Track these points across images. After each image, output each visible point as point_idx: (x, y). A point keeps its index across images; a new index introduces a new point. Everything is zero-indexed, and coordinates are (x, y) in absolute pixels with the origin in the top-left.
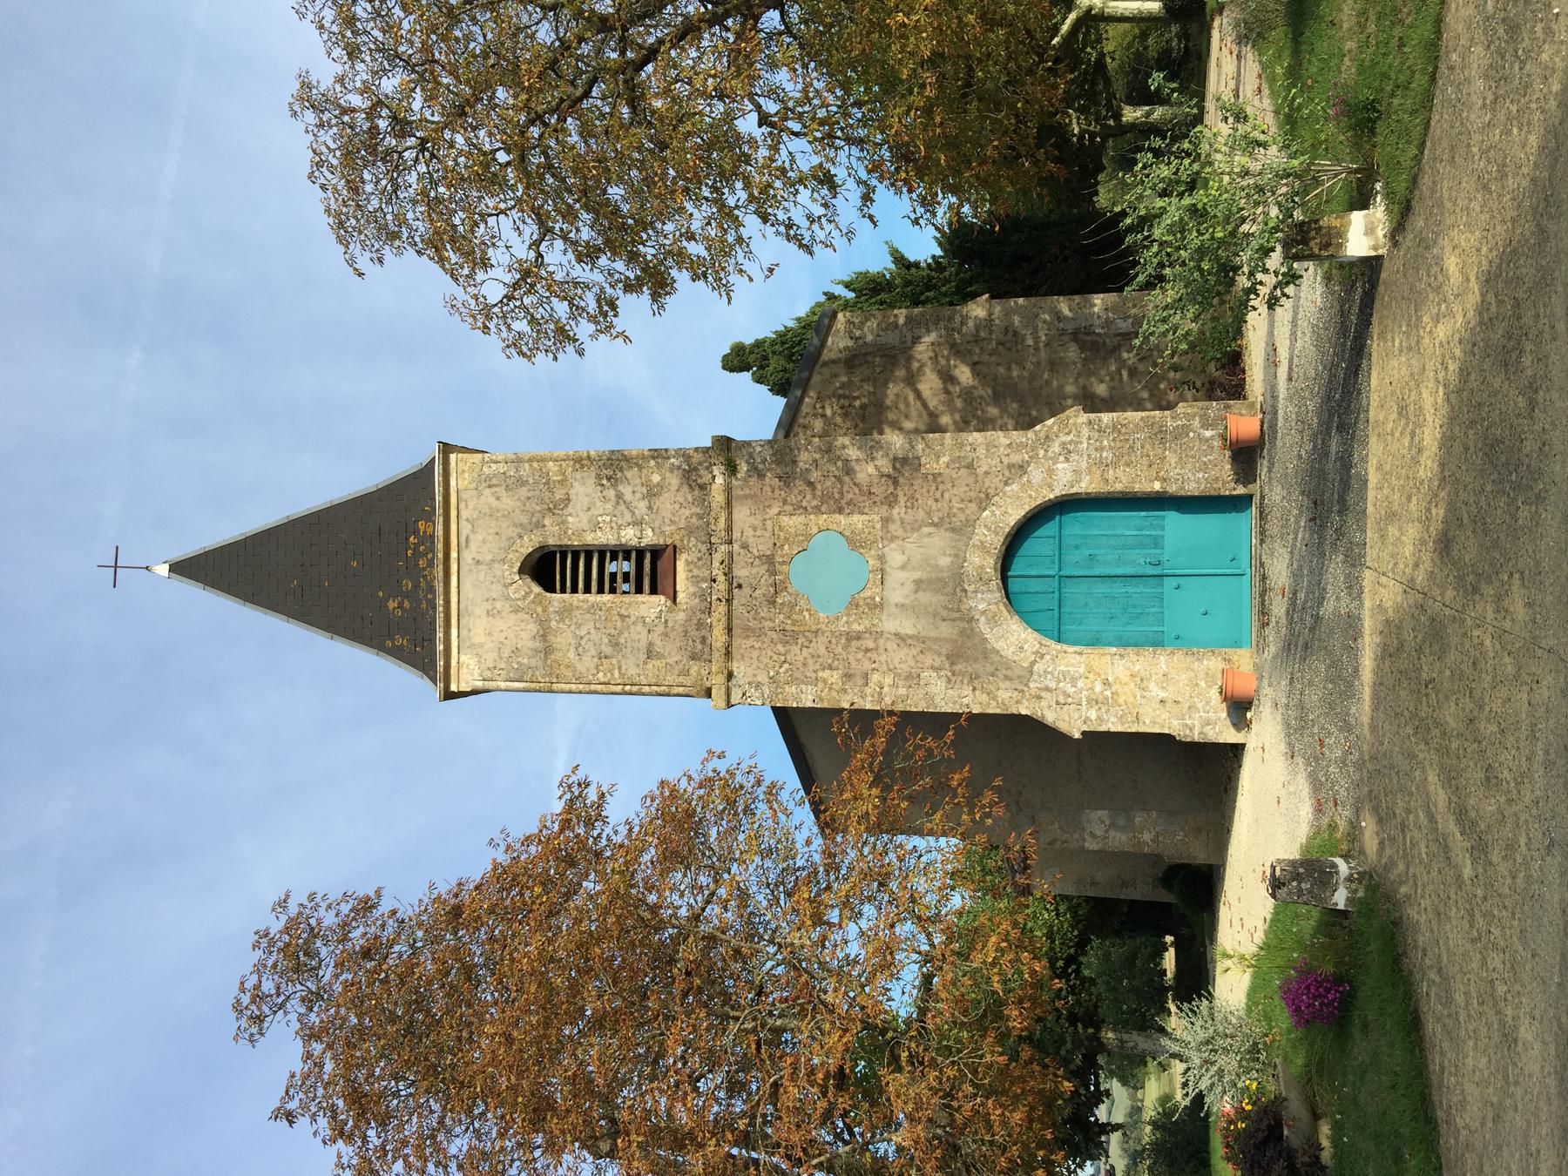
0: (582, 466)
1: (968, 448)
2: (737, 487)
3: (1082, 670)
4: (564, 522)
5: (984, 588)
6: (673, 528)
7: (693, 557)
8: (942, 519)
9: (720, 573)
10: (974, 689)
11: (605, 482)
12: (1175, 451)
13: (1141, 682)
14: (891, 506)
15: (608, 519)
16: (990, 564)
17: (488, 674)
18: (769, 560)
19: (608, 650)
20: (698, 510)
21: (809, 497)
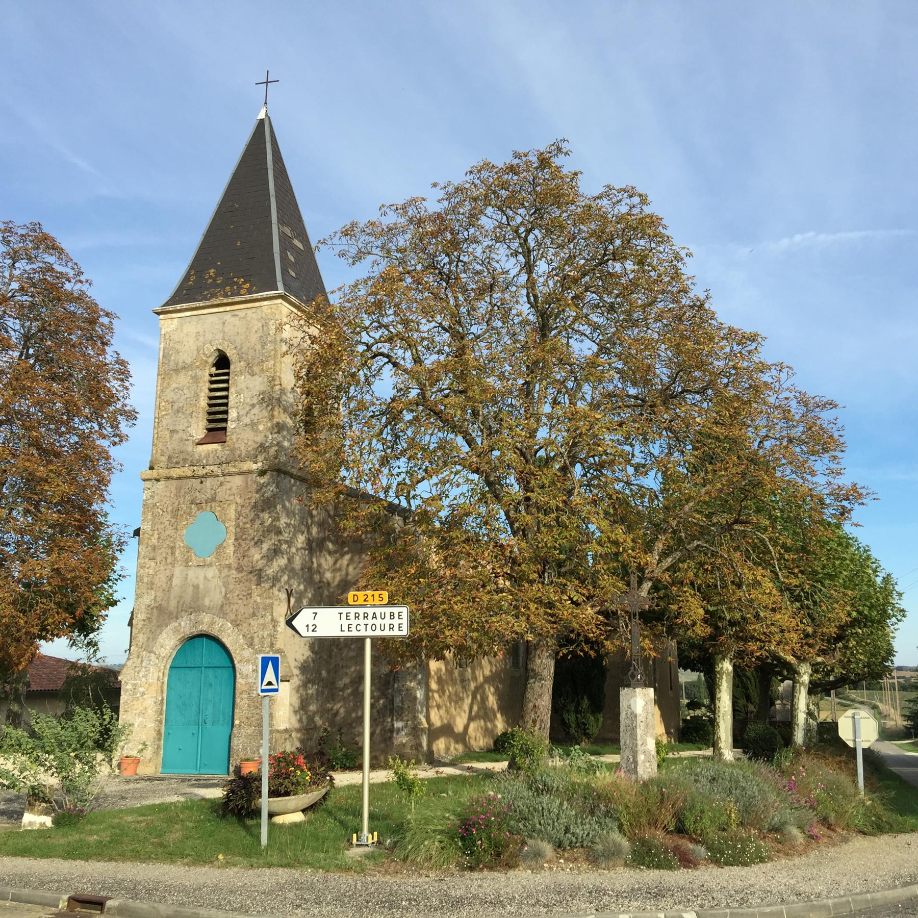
0: (270, 382)
1: (263, 613)
2: (252, 477)
3: (150, 681)
4: (241, 374)
5: (192, 625)
6: (235, 440)
7: (219, 454)
8: (228, 599)
9: (207, 471)
10: (144, 620)
11: (261, 396)
12: (254, 732)
13: (142, 714)
14: (237, 569)
15: (242, 400)
16: (204, 628)
17: (167, 337)
18: (213, 499)
19: (175, 407)
20: (243, 454)
21: (244, 520)
